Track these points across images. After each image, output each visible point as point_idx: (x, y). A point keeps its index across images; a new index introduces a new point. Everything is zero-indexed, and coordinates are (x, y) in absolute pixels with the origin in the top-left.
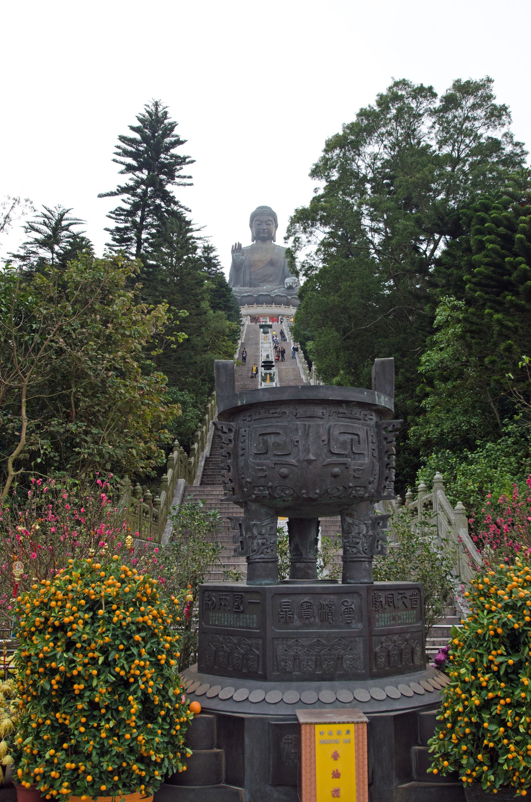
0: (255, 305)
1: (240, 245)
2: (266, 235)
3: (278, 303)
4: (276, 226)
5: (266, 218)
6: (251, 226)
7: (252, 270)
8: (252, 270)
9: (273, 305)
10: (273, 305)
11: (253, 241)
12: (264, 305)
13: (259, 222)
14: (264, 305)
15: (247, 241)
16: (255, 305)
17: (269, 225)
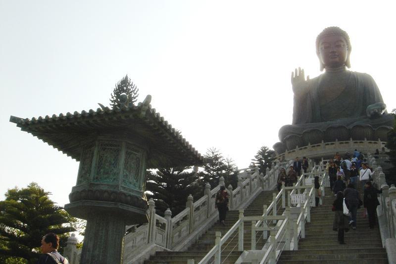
1: (302, 72)
2: (337, 59)
3: (359, 138)
4: (349, 49)
9: (351, 142)
11: (322, 70)
12: (337, 143)
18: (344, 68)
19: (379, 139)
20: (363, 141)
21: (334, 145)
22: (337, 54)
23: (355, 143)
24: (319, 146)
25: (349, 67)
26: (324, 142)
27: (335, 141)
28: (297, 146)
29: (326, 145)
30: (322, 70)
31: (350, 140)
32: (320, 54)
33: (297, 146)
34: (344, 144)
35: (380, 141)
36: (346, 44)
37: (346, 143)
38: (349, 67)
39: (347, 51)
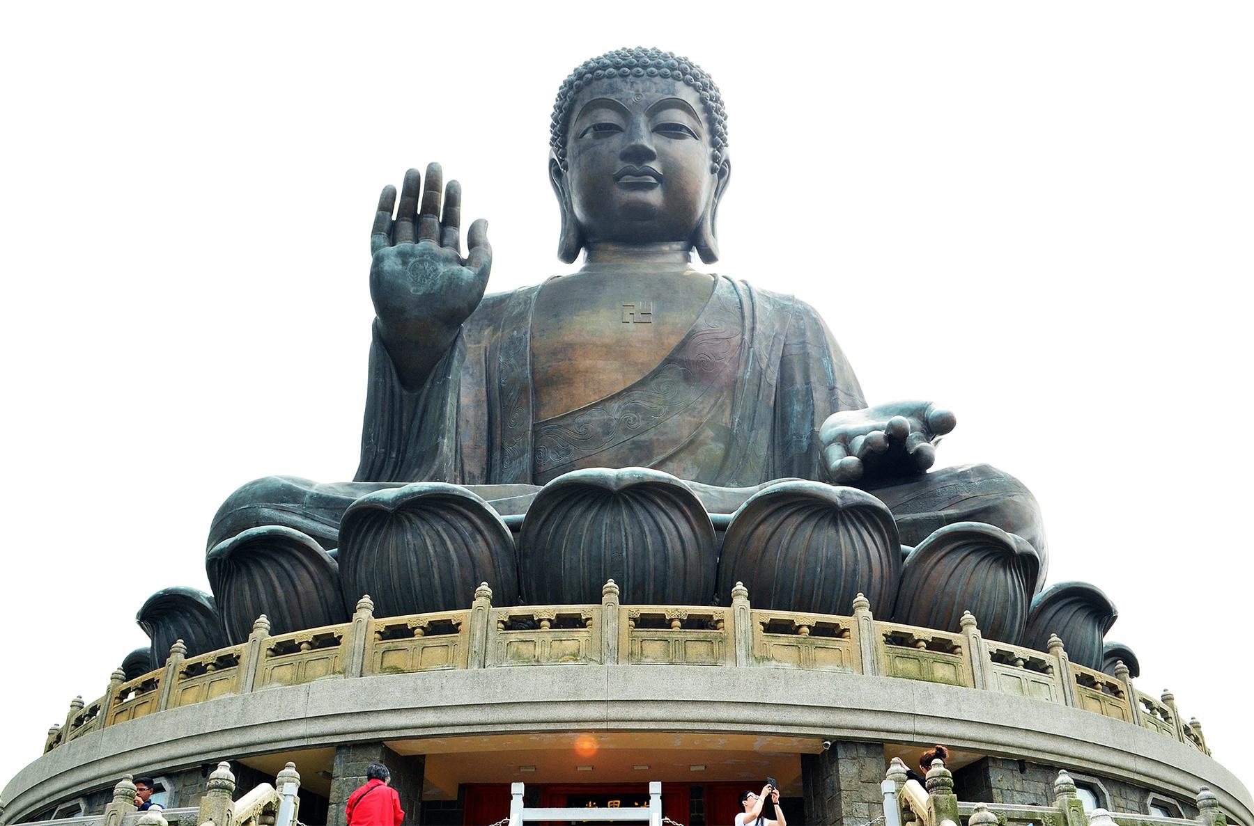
0: (481, 615)
2: (655, 197)
4: (721, 171)
5: (655, 91)
6: (557, 172)
7: (547, 415)
8: (547, 415)
9: (741, 615)
10: (741, 615)
11: (568, 255)
12: (612, 614)
13: (608, 117)
14: (612, 614)
15: (521, 240)
16: (481, 615)
17: (673, 131)
18: (688, 259)
19: (968, 616)
20: (841, 620)
21: (581, 634)
22: (655, 166)
23: (773, 628)
24: (448, 628)
25: (708, 257)
26: (497, 602)
27: (596, 598)
28: (263, 620)
29: (513, 624)
30: (568, 255)
31: (728, 602)
32: (572, 176)
33: (263, 620)
34: (676, 632)
35: (974, 631)
36: (706, 138)
37: (692, 623)
38: (708, 257)
39: (705, 183)
